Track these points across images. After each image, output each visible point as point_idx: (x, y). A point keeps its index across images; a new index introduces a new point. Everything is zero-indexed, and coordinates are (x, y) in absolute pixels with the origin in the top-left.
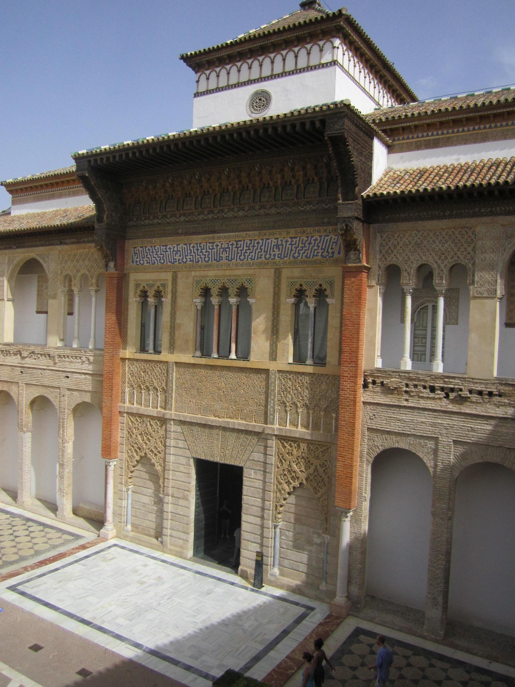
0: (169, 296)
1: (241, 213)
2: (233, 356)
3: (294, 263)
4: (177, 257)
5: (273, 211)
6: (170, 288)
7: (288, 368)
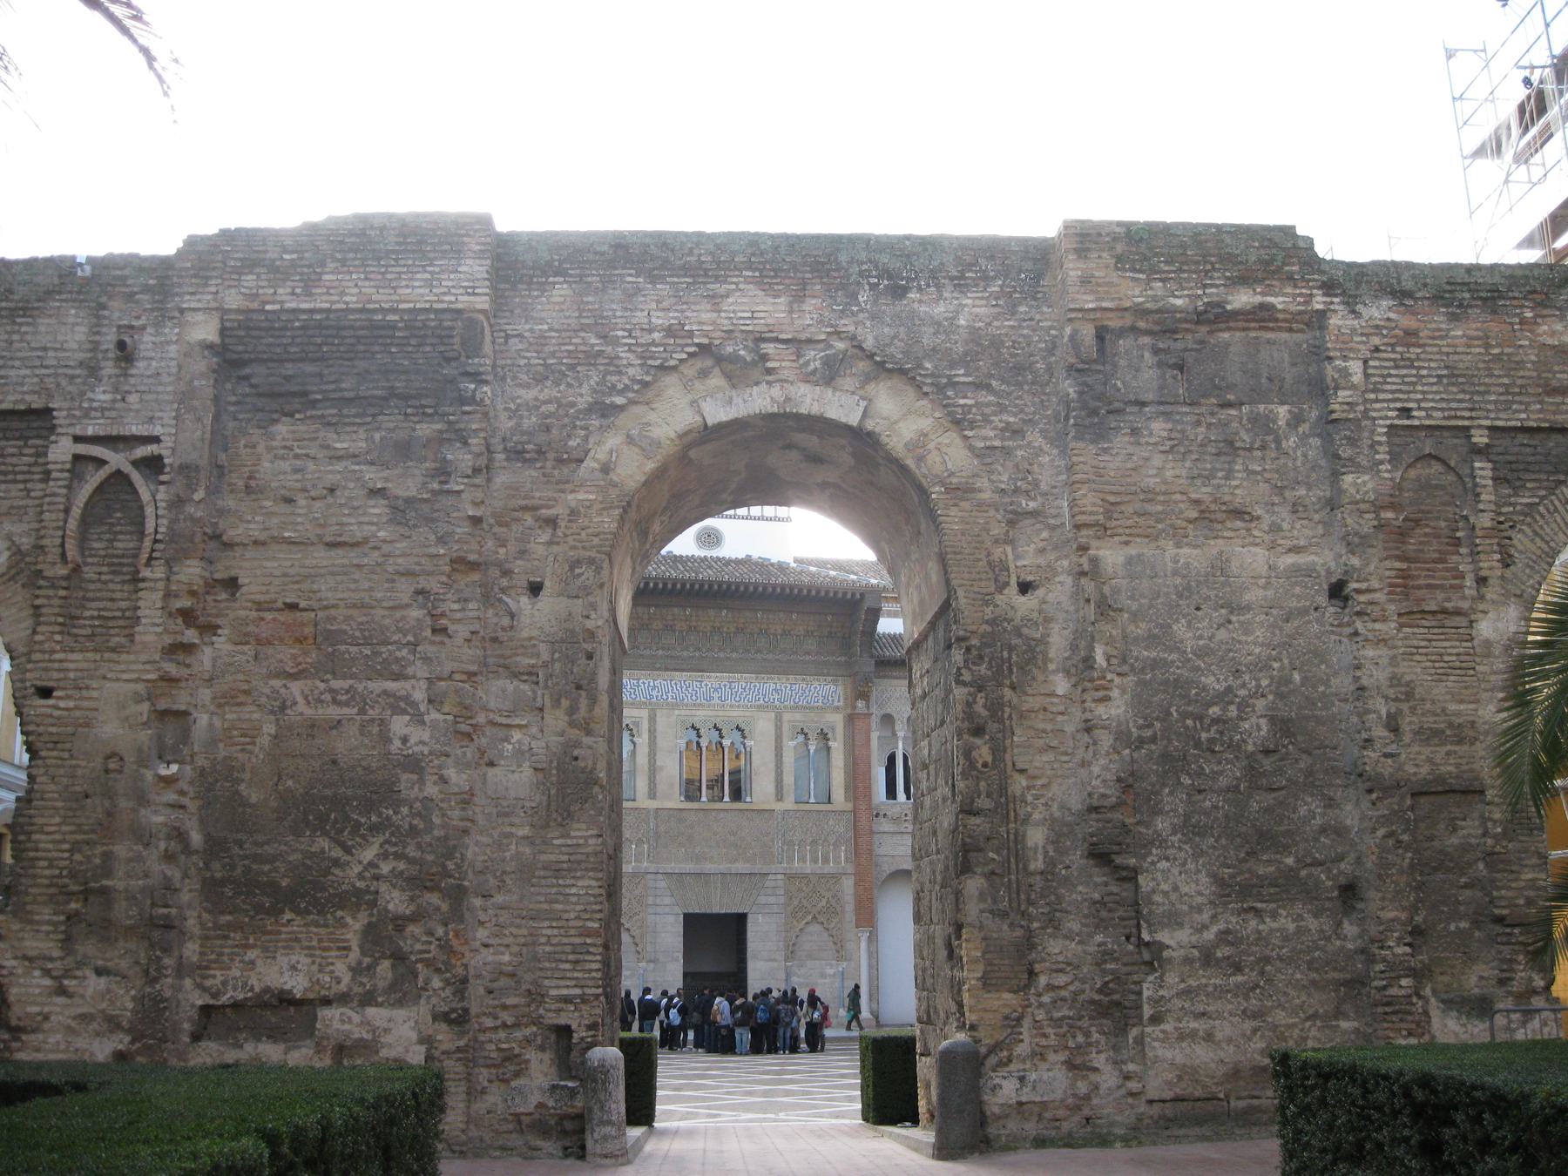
0: (646, 736)
1: (734, 655)
2: (727, 799)
3: (796, 708)
4: (654, 693)
5: (770, 656)
6: (645, 726)
7: (796, 807)
